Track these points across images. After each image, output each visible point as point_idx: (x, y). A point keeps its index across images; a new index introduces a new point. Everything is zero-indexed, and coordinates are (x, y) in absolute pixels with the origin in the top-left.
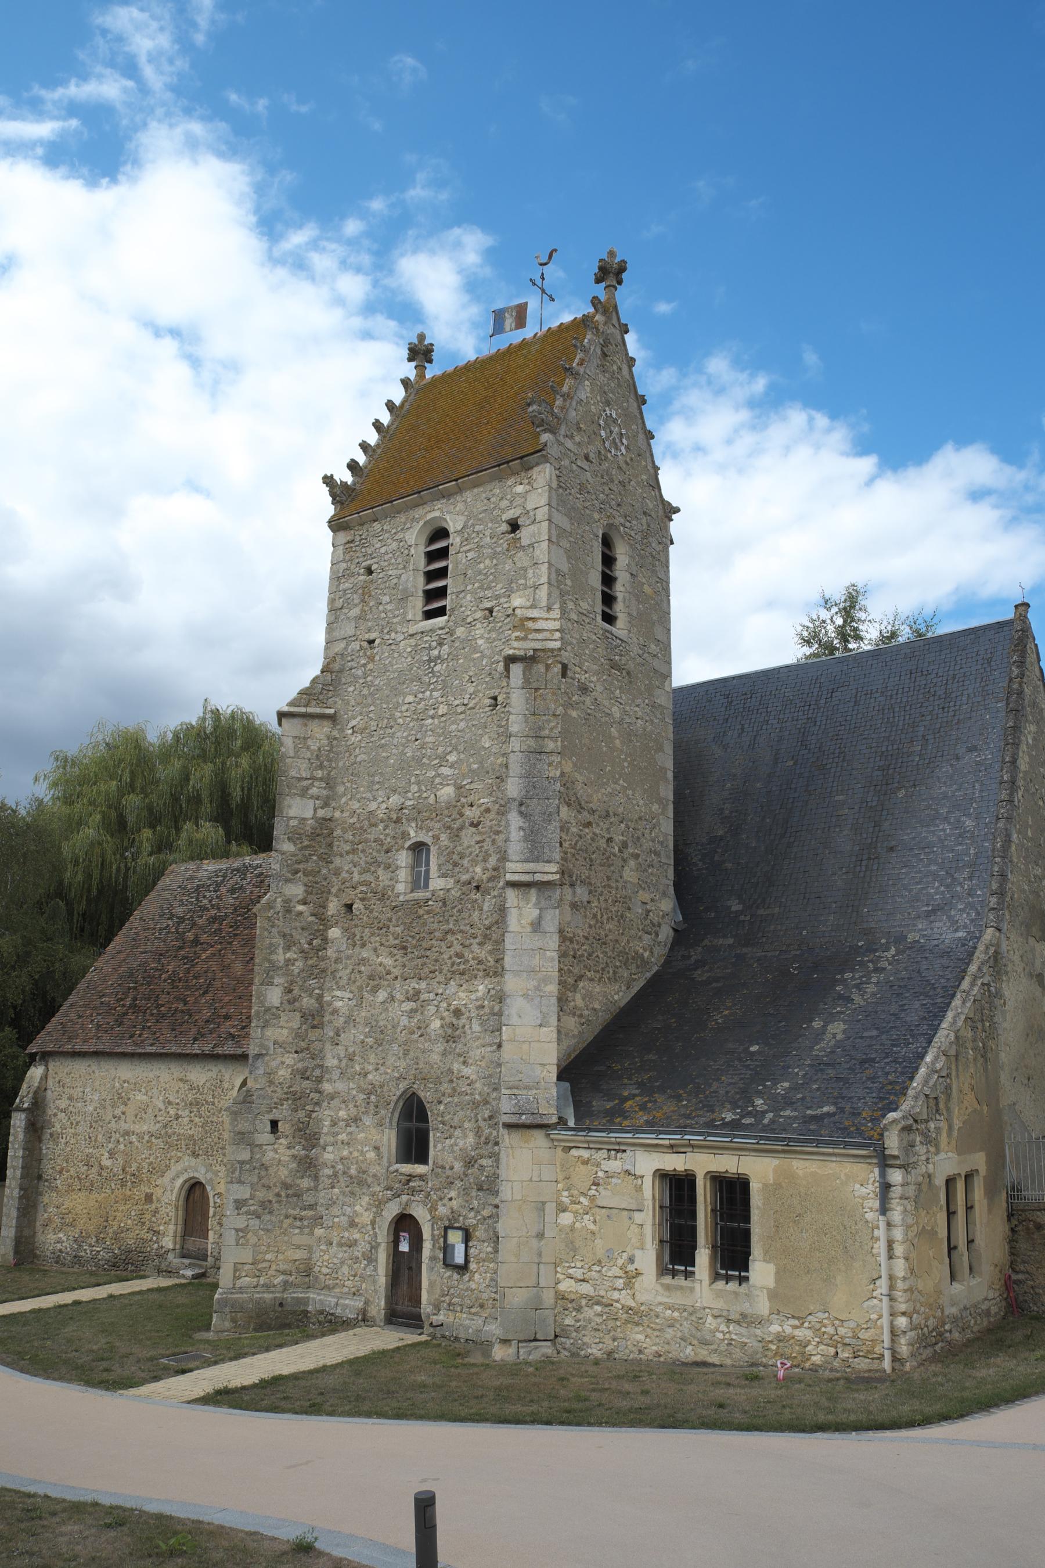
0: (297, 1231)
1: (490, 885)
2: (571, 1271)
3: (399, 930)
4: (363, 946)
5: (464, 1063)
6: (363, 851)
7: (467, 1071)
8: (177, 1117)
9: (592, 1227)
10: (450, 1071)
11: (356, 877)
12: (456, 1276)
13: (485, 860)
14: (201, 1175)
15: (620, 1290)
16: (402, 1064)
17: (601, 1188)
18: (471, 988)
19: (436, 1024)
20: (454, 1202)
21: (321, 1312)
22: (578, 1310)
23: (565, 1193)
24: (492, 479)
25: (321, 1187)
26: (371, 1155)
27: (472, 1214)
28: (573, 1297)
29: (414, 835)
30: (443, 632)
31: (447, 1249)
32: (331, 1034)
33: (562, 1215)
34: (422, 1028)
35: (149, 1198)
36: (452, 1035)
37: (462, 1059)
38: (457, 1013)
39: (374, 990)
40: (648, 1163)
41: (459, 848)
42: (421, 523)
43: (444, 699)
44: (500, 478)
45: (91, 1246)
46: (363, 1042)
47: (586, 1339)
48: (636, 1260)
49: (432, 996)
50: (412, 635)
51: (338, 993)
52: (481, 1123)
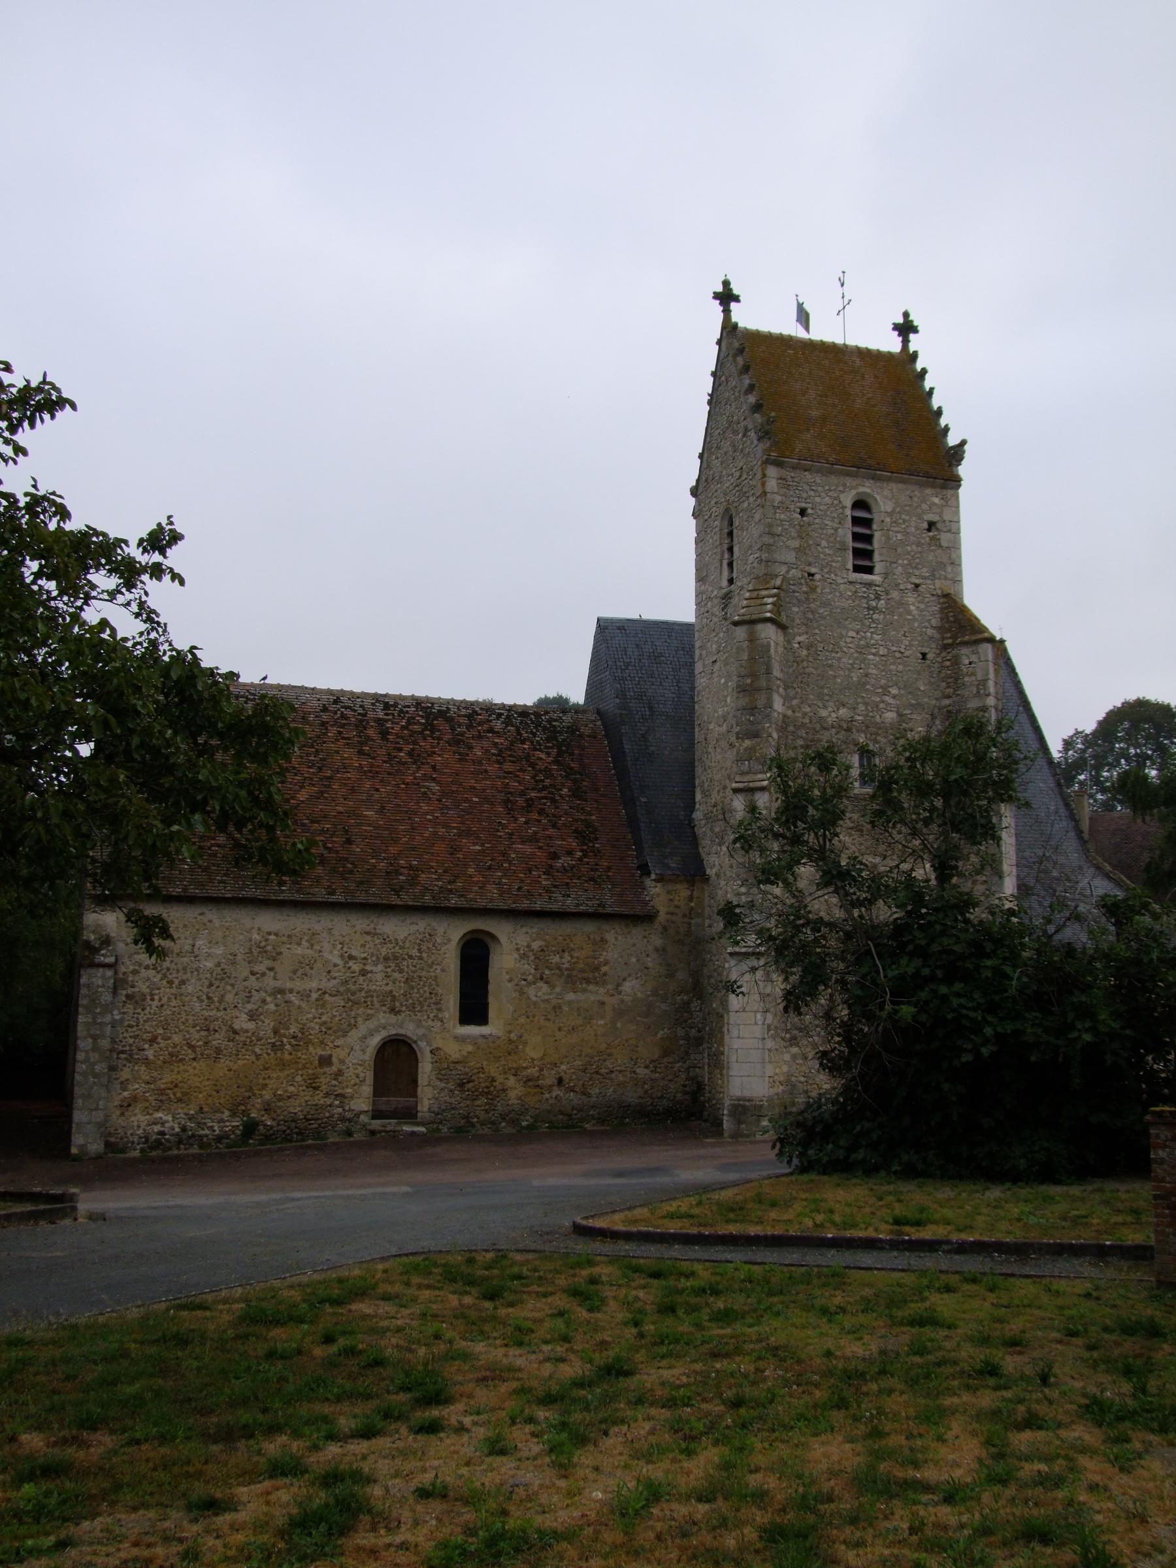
8: (364, 973)
14: (409, 1030)
24: (917, 483)
35: (325, 1061)
44: (922, 485)
45: (221, 1121)
50: (851, 583)
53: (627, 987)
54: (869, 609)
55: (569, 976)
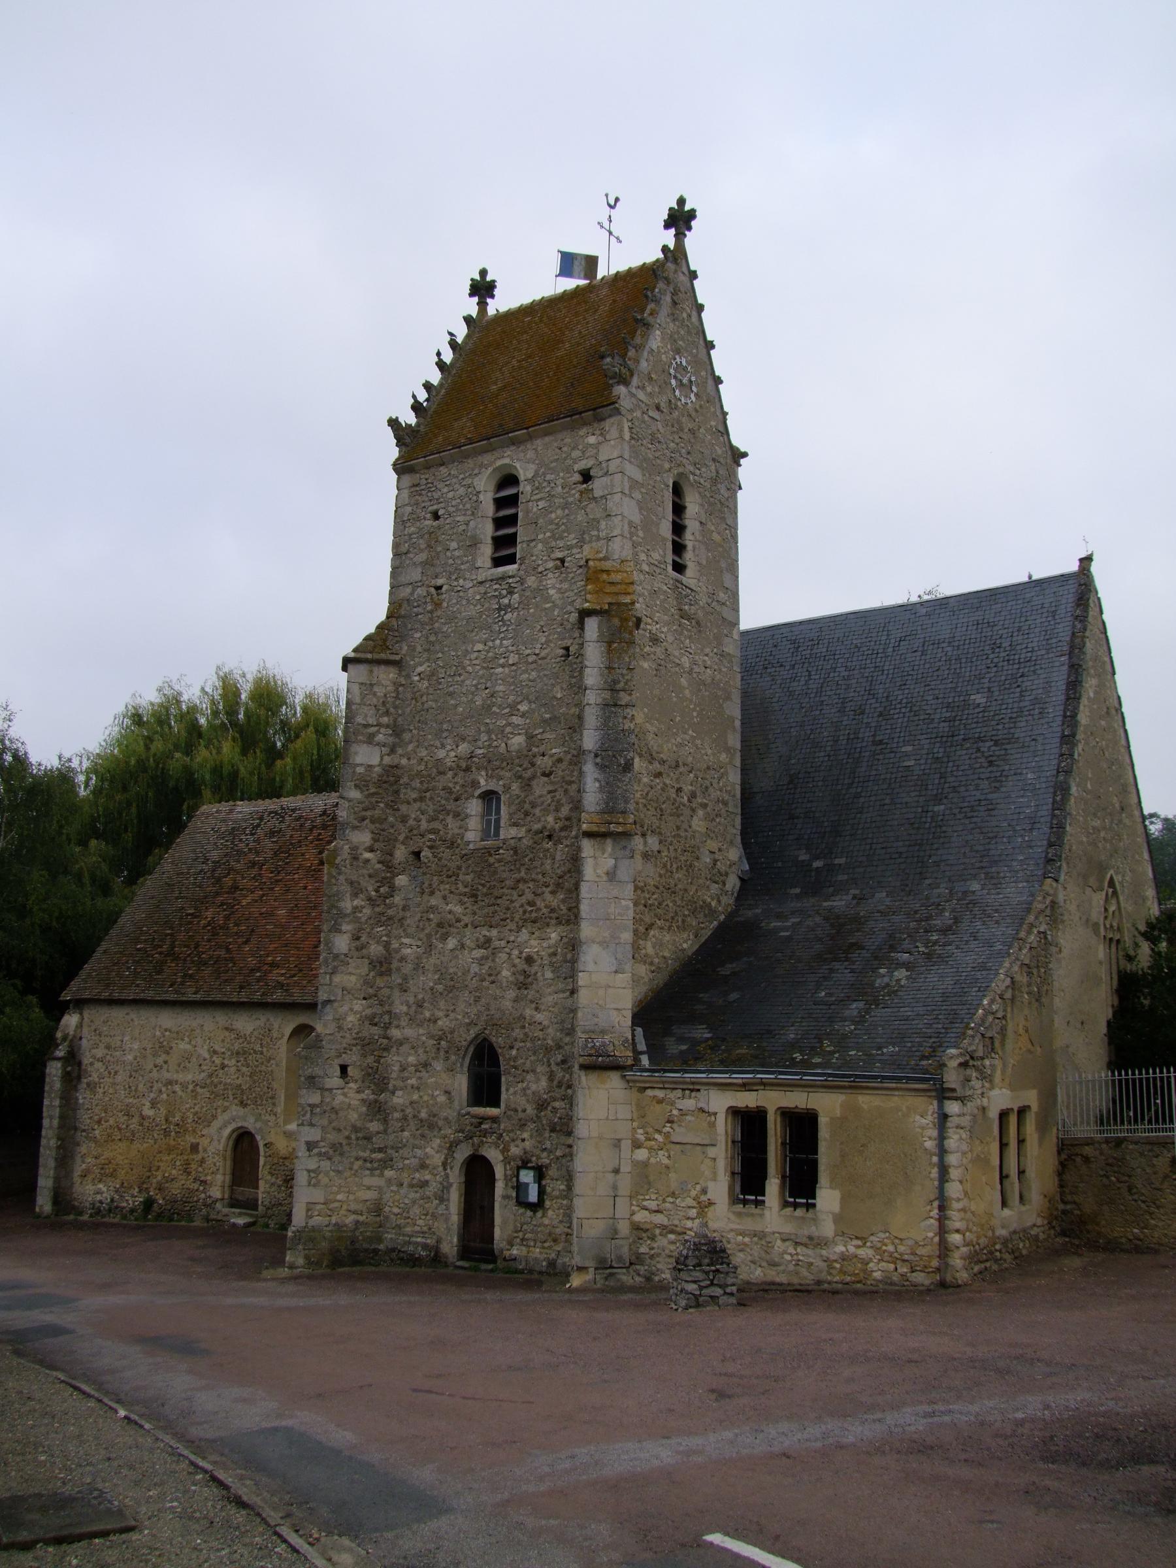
0: (368, 1172)
1: (563, 834)
2: (645, 1203)
3: (469, 878)
4: (432, 893)
5: (537, 1009)
6: (431, 798)
7: (539, 1017)
8: (223, 1067)
9: (666, 1161)
11: (424, 825)
12: (529, 1213)
13: (557, 810)
14: (250, 1124)
15: (693, 1219)
16: (473, 1010)
17: (675, 1126)
18: (543, 936)
20: (527, 1143)
21: (393, 1250)
22: (653, 1238)
23: (640, 1131)
25: (390, 1130)
26: (442, 1099)
27: (545, 1154)
28: (648, 1226)
29: (484, 784)
30: (514, 580)
31: (520, 1188)
32: (399, 981)
33: (637, 1151)
35: (195, 1148)
36: (524, 982)
37: (533, 1006)
38: (529, 960)
39: (444, 938)
40: (720, 1102)
41: (531, 798)
42: (490, 470)
43: (514, 648)
44: (572, 428)
45: (133, 1196)
46: (432, 989)
47: (659, 1266)
48: (709, 1191)
49: (503, 943)
52: (554, 1068)
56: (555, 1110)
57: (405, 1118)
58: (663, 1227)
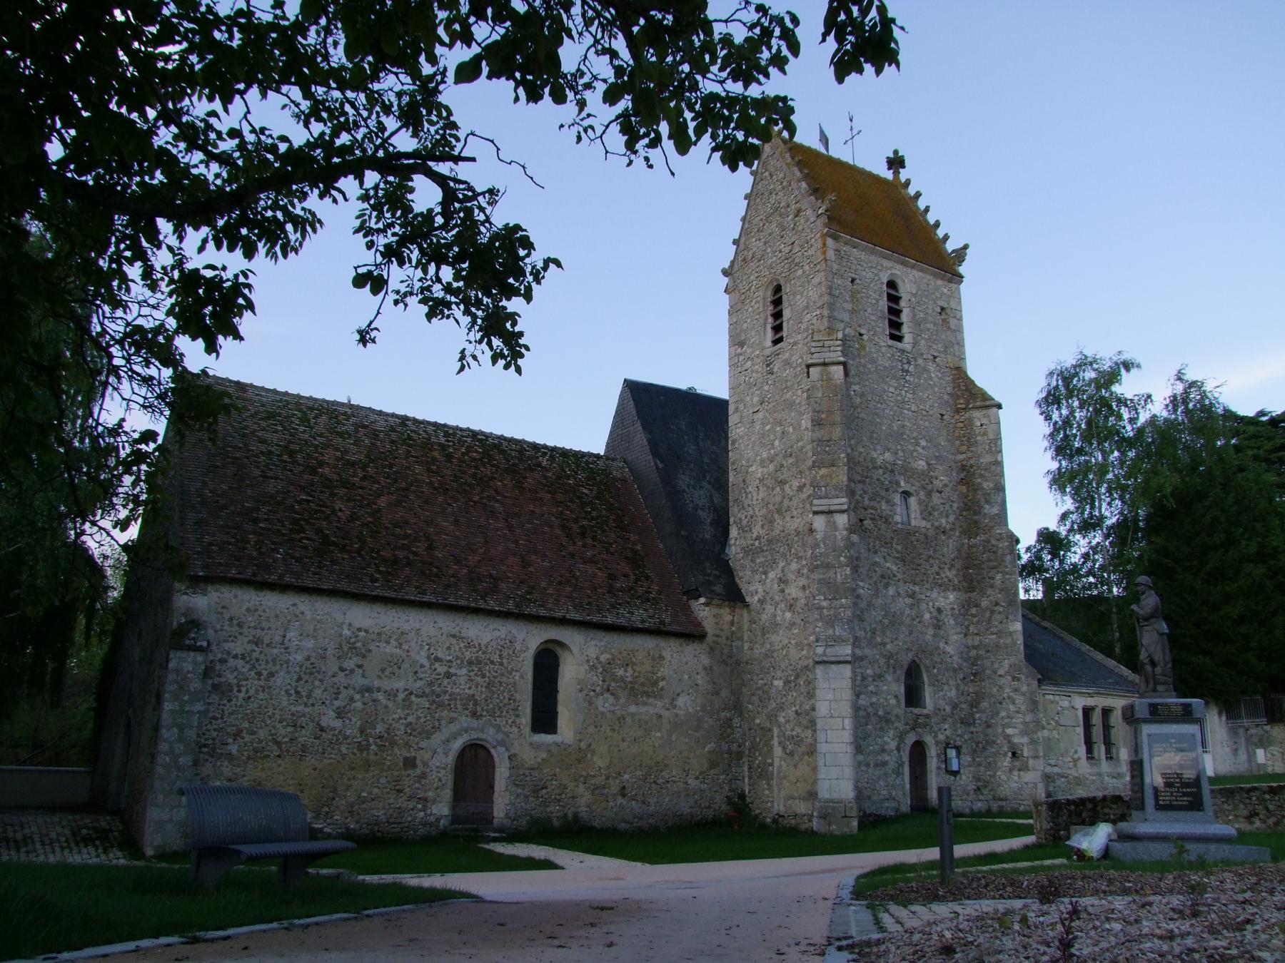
3: (899, 547)
4: (876, 552)
7: (948, 649)
8: (448, 675)
10: (938, 648)
11: (867, 502)
13: (947, 516)
14: (489, 736)
19: (927, 616)
26: (893, 701)
34: (920, 616)
35: (410, 763)
38: (939, 610)
39: (886, 586)
40: (1080, 702)
51: (861, 584)
53: (680, 702)
54: (903, 370)
55: (632, 689)
56: (962, 710)
57: (868, 715)
58: (1058, 774)
